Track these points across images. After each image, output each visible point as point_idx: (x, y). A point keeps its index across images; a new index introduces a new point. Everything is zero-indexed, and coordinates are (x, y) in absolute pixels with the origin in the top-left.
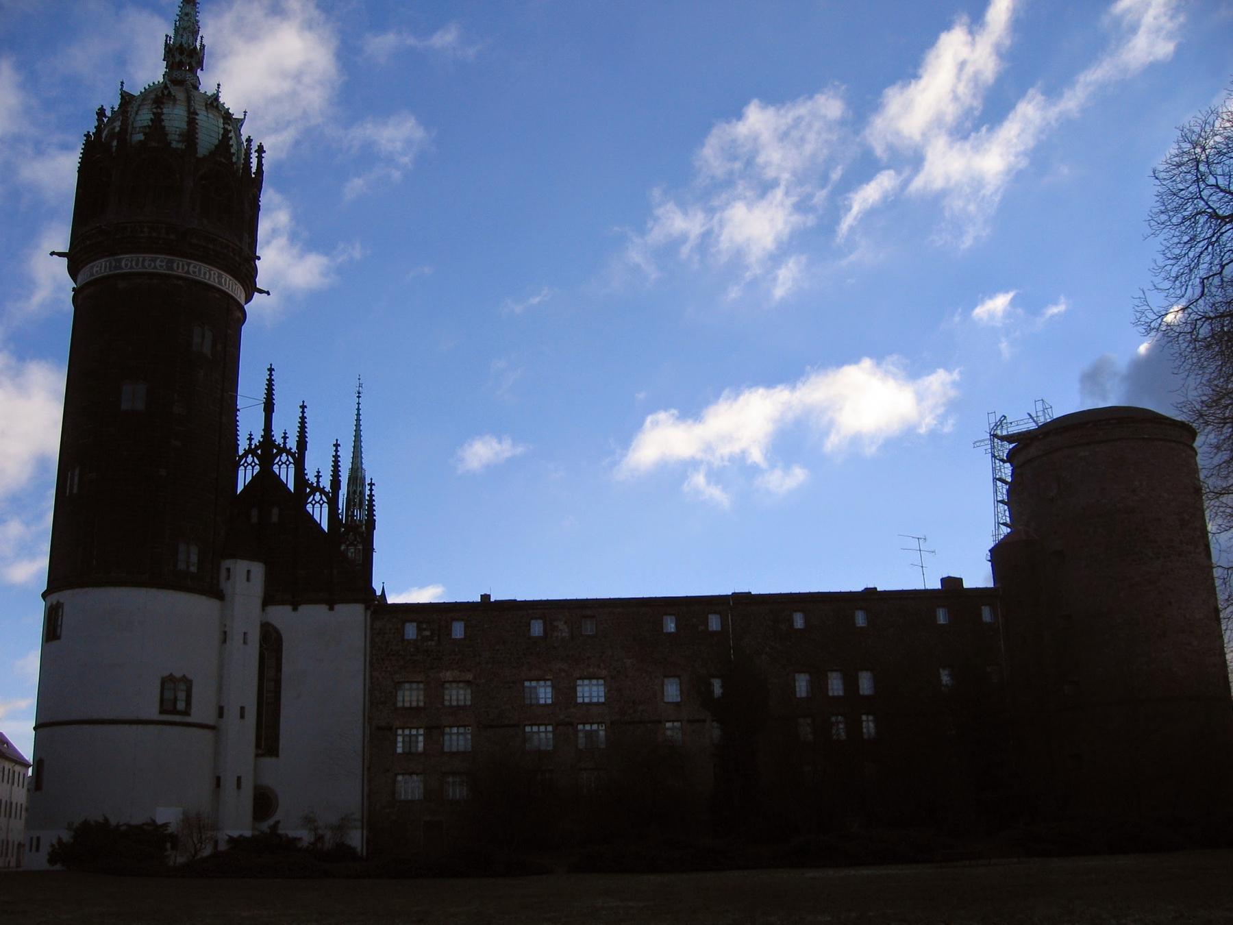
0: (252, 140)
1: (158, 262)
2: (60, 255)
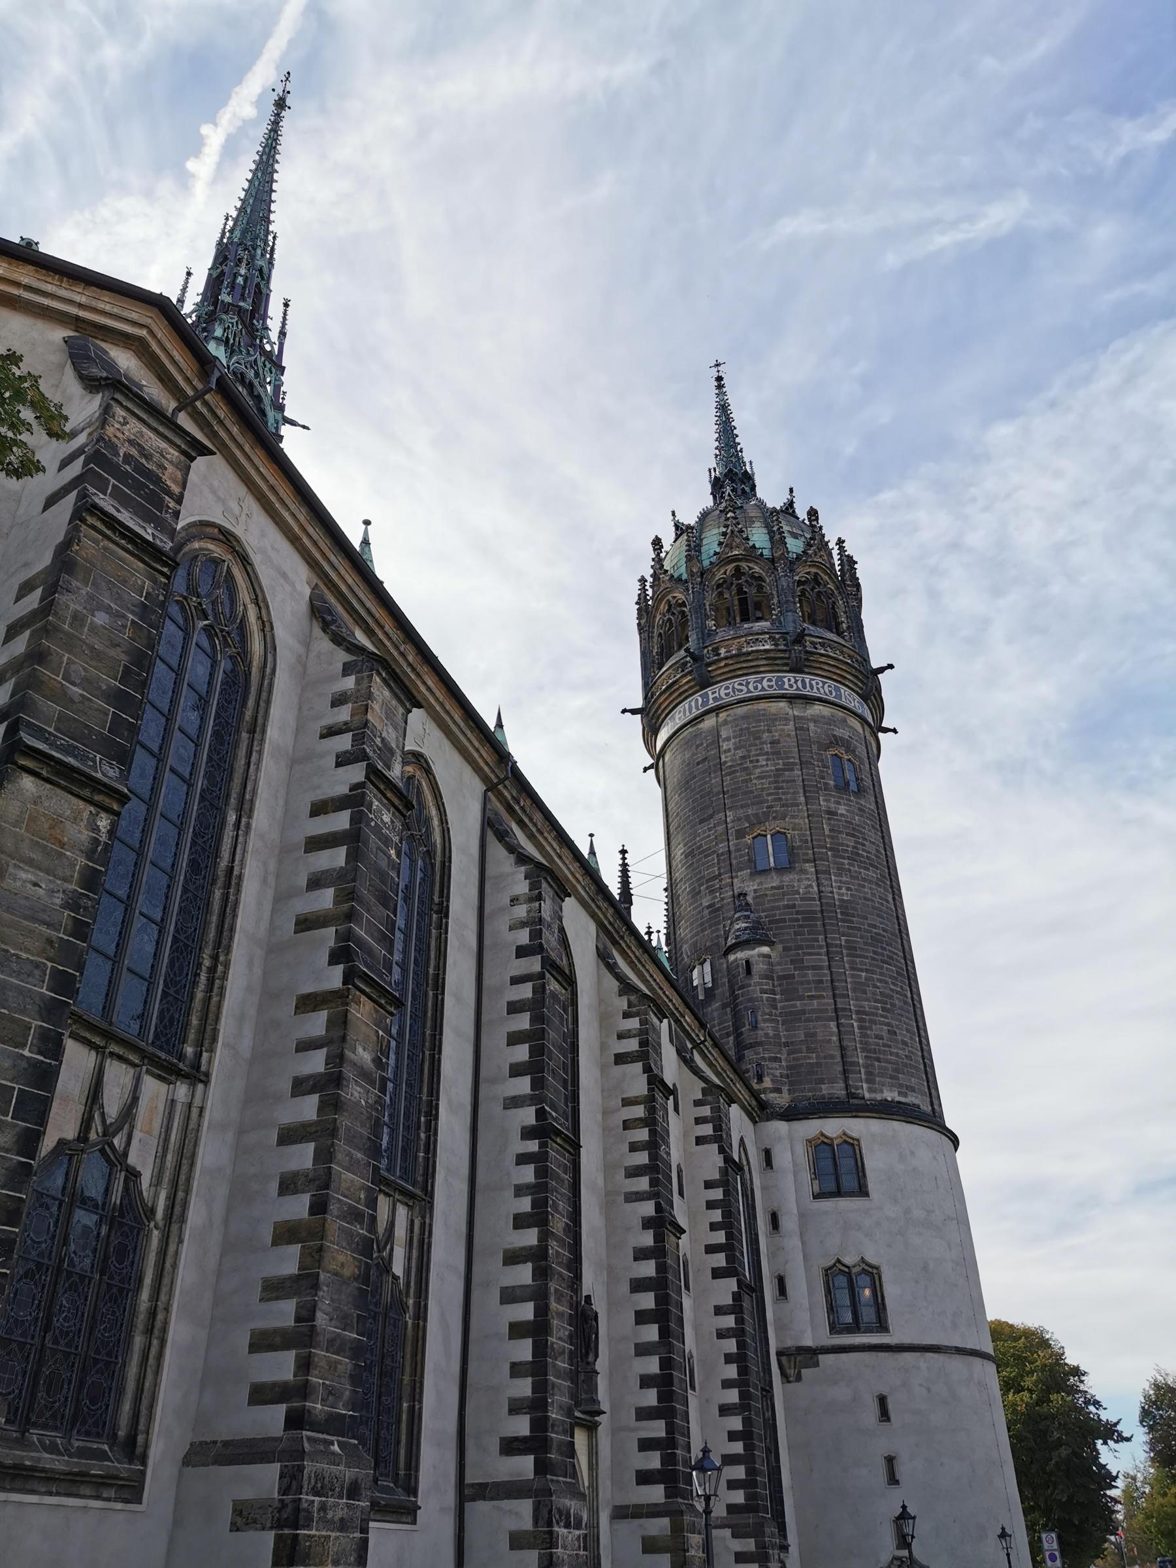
0: (844, 541)
1: (765, 683)
2: (634, 712)
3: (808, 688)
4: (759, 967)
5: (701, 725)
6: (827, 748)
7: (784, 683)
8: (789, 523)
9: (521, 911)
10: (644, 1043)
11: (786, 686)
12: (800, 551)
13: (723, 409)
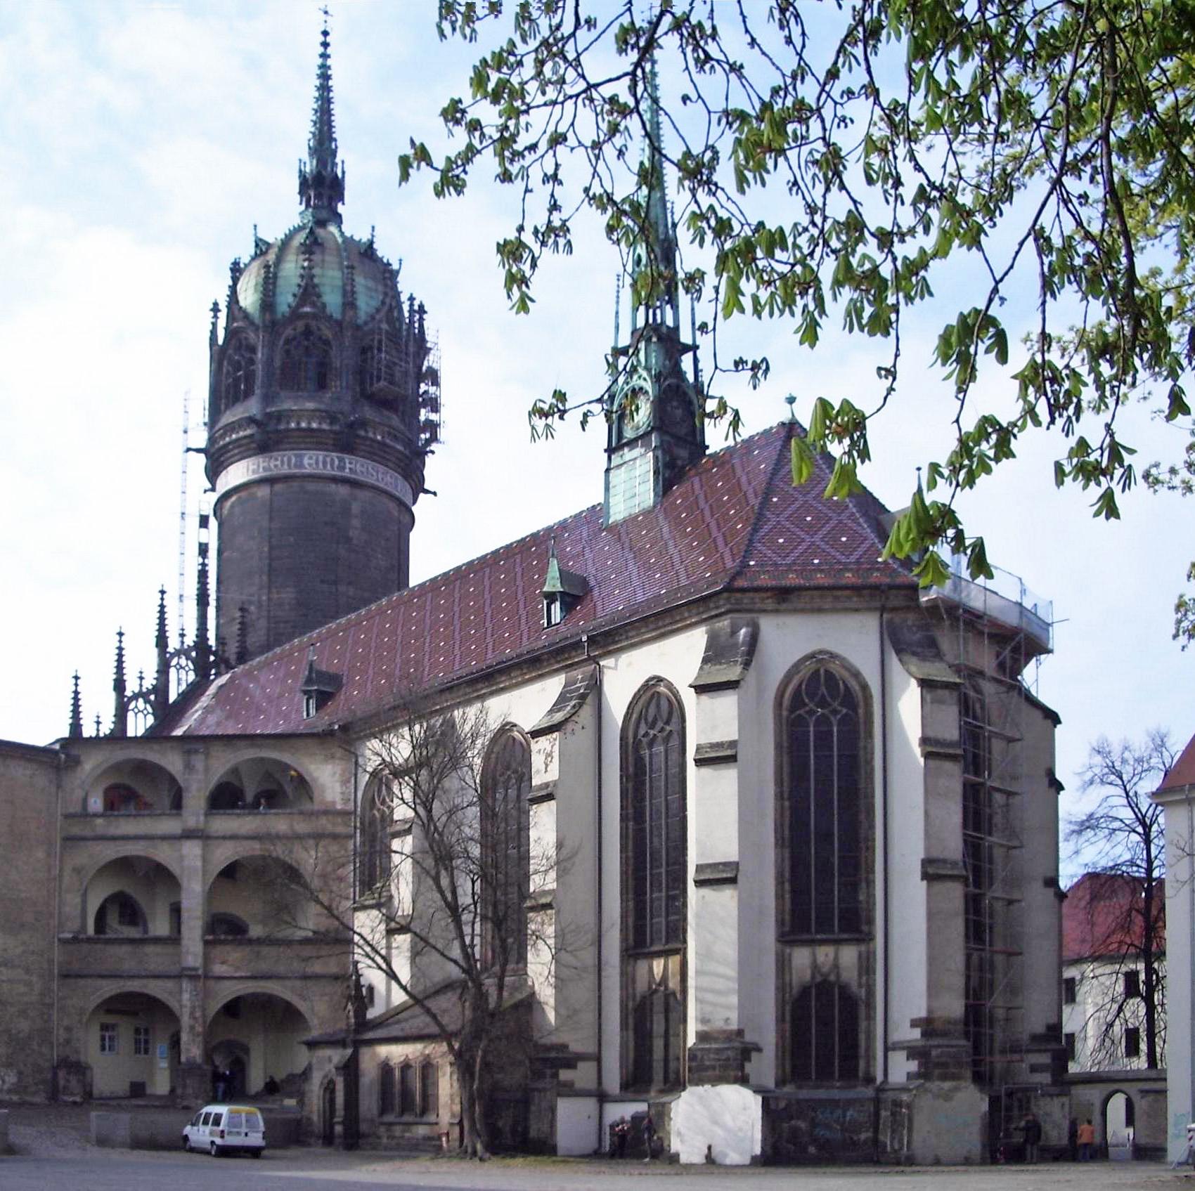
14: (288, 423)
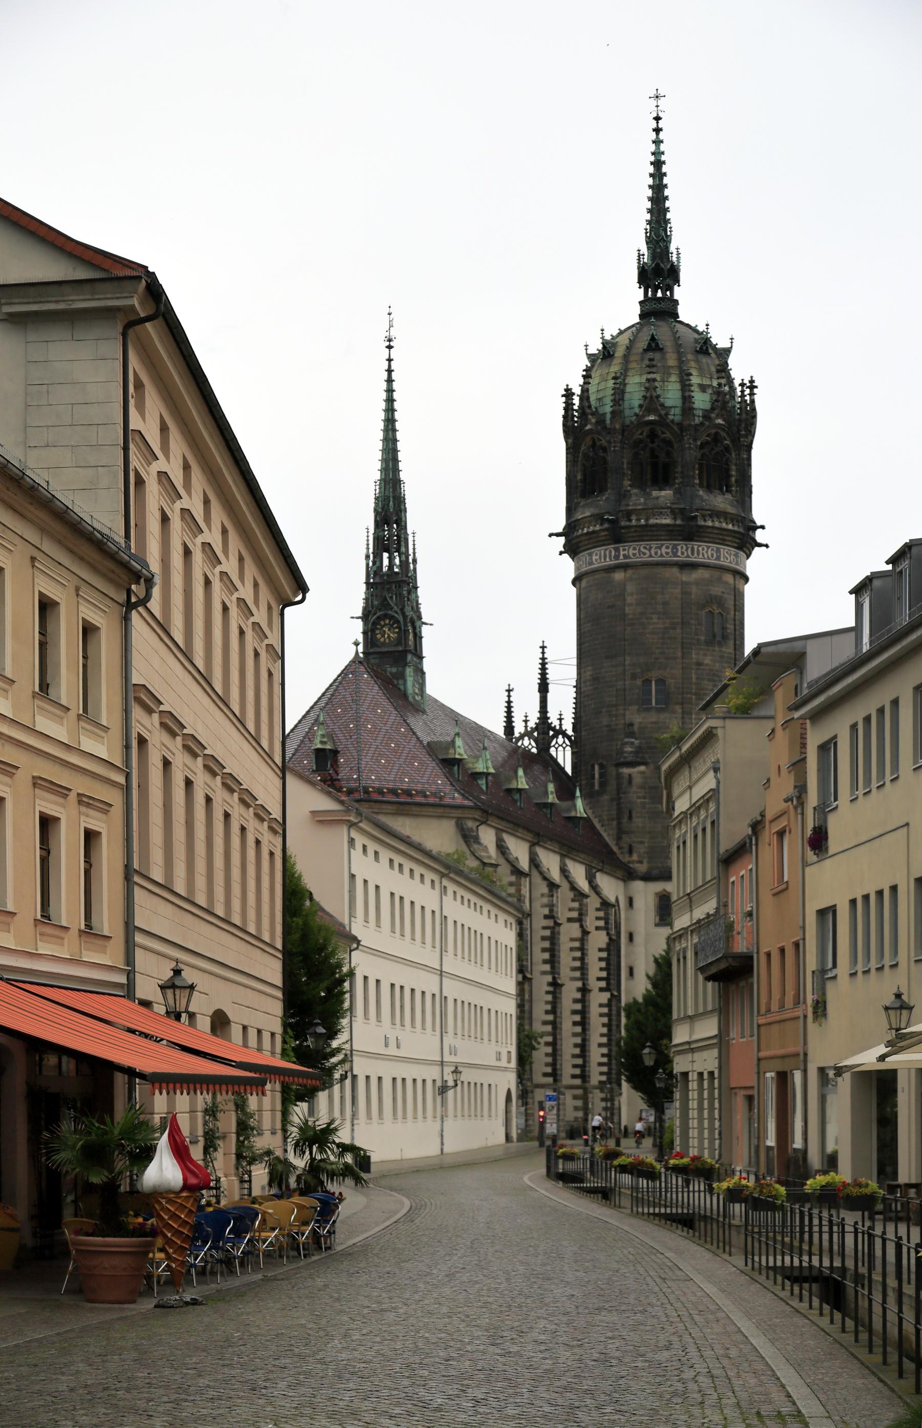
1: (664, 550)
2: (558, 535)
3: (696, 555)
4: (637, 780)
5: (612, 575)
6: (703, 607)
7: (677, 550)
8: (701, 375)
9: (545, 900)
10: (580, 914)
11: (679, 554)
12: (708, 406)
13: (658, 164)
14: (639, 520)
